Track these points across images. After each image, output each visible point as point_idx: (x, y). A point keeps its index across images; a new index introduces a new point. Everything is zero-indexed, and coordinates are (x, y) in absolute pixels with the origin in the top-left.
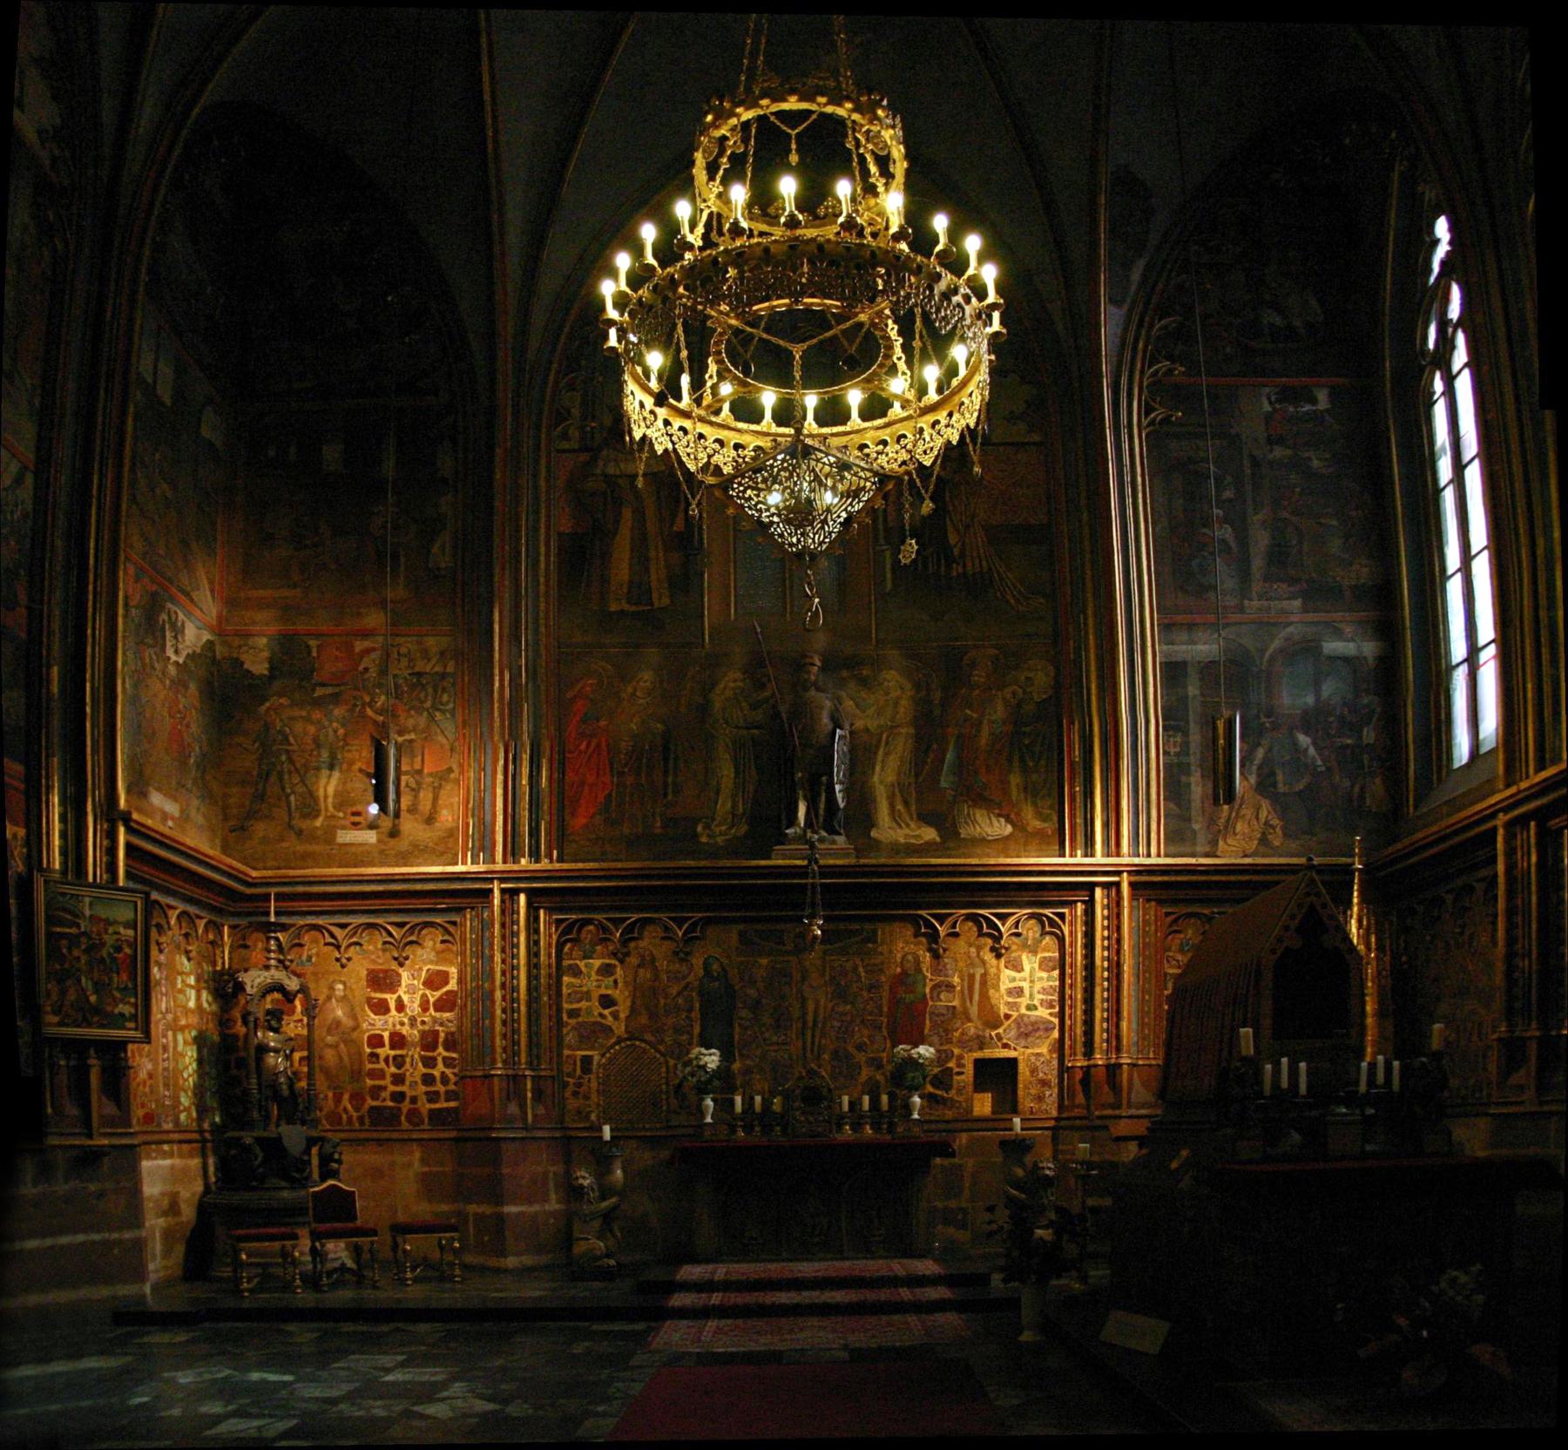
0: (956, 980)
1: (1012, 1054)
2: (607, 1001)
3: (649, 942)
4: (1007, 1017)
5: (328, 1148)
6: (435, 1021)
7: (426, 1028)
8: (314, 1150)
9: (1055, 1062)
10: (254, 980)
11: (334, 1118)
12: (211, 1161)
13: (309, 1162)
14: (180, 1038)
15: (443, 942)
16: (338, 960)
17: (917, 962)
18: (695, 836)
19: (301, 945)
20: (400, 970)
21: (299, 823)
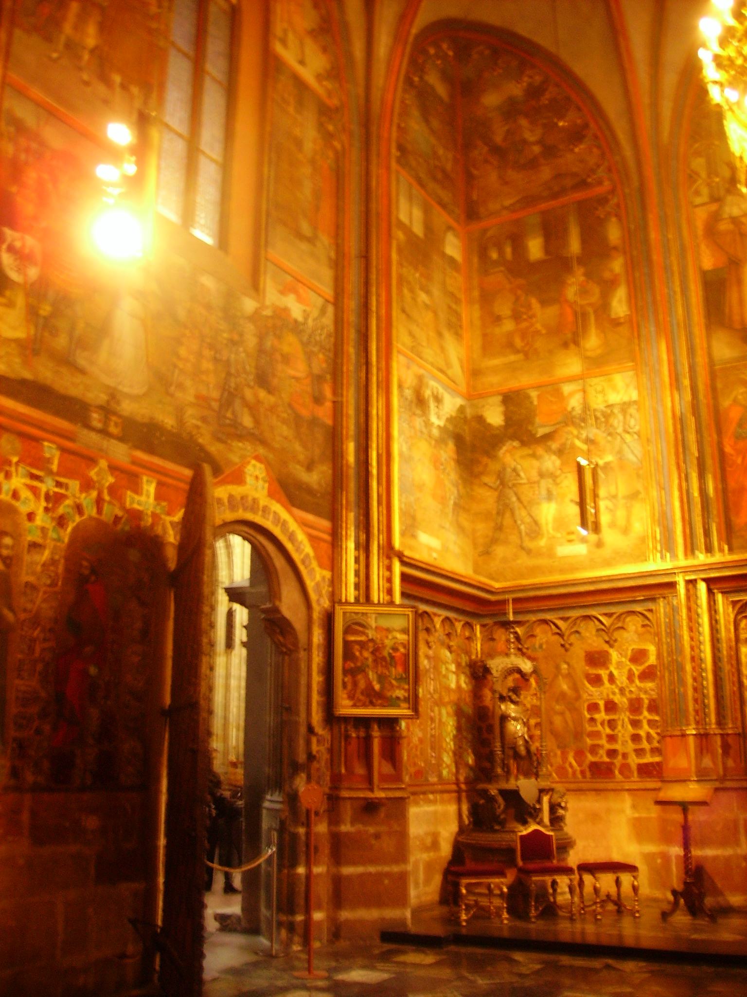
5: (556, 798)
6: (640, 689)
7: (634, 696)
8: (546, 799)
10: (497, 665)
11: (561, 771)
12: (465, 807)
13: (540, 810)
14: (444, 711)
15: (643, 626)
16: (562, 646)
19: (533, 636)
20: (611, 651)
21: (528, 544)
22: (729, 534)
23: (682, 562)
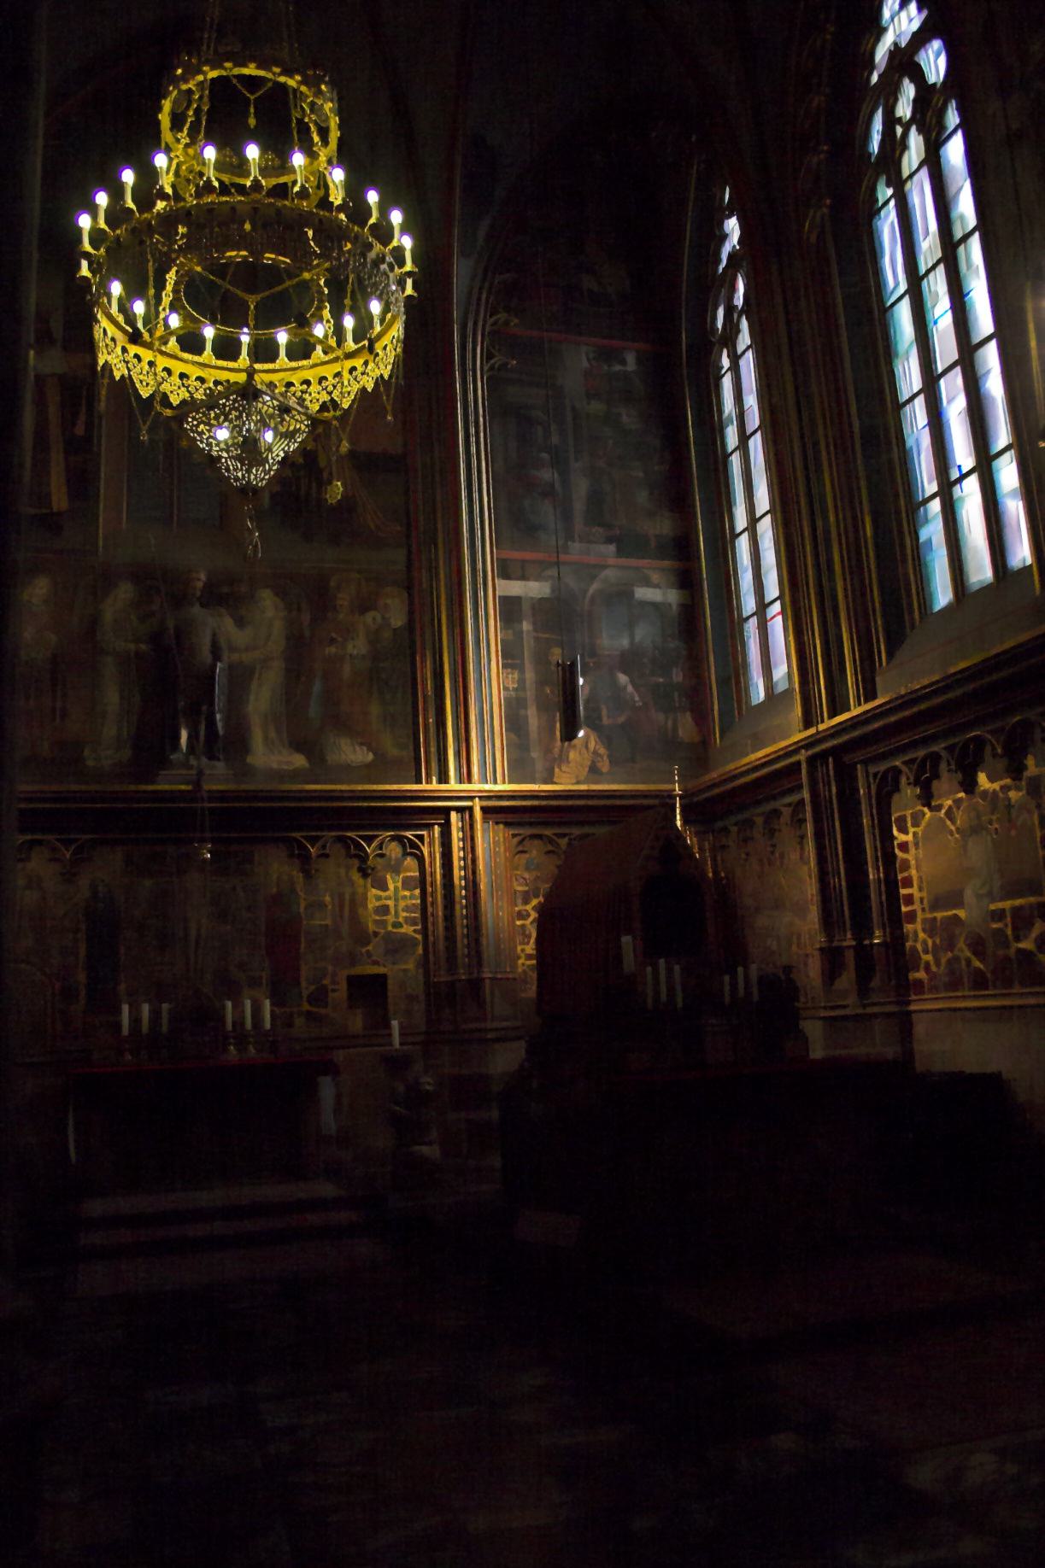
0: (328, 899)
1: (381, 970)
4: (376, 934)
9: (421, 978)
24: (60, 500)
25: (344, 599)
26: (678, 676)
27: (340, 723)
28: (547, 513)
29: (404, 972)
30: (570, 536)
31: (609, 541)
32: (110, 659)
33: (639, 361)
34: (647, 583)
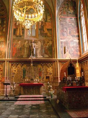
2: (15, 71)
3: (19, 66)
17: (41, 68)
18: (23, 57)
22: (12, 56)
23: (6, 59)
24: (21, 34)
25: (46, 42)
26: (78, 48)
27: (46, 53)
28: (65, 33)
29: (51, 76)
30: (67, 35)
31: (71, 36)
32: (25, 48)
33: (74, 18)
34: (75, 40)
